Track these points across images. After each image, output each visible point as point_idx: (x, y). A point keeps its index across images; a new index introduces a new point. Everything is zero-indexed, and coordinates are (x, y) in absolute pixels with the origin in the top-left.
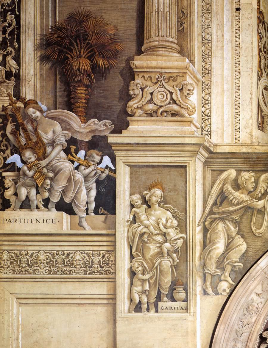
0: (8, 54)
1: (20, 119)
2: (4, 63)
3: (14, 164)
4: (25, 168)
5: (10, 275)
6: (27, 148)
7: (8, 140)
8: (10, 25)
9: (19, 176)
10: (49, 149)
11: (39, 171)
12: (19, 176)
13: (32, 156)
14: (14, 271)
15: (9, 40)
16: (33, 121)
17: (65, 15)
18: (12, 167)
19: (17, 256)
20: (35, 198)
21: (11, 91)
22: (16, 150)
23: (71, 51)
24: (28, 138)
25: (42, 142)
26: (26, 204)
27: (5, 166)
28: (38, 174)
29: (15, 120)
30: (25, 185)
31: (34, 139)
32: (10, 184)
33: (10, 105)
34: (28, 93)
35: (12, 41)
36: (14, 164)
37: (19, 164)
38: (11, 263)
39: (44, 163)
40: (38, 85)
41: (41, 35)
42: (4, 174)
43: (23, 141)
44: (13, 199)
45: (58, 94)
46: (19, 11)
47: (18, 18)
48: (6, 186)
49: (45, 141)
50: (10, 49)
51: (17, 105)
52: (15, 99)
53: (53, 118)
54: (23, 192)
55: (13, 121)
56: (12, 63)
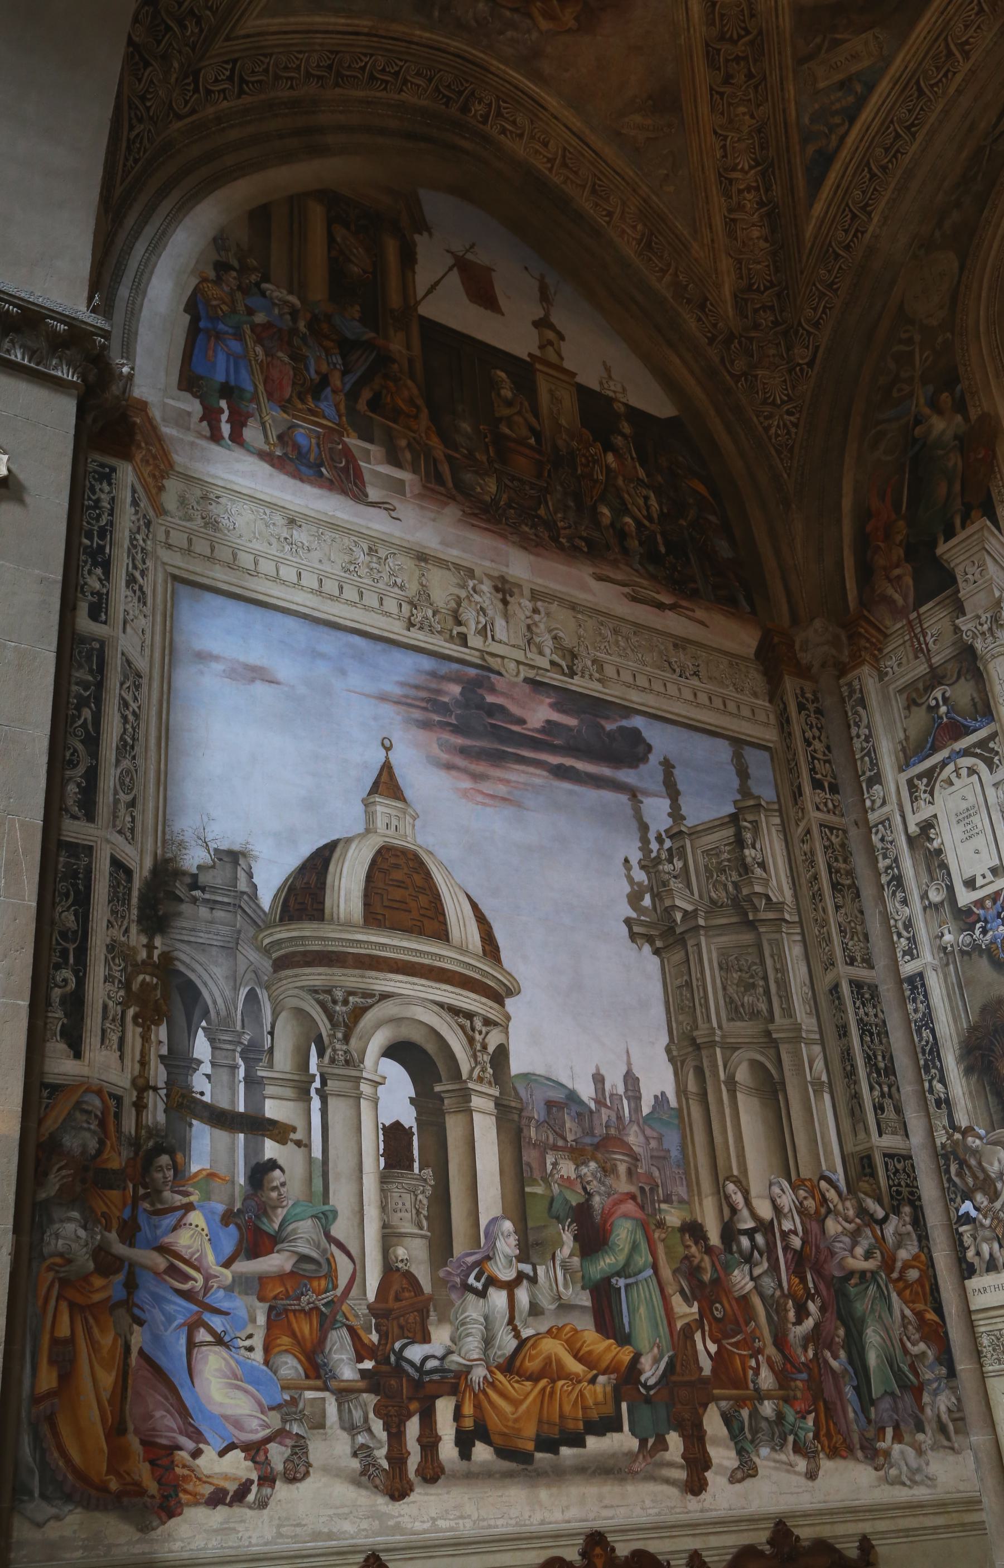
0: (933, 1078)
1: (961, 1156)
2: (931, 1090)
3: (967, 1213)
4: (981, 1217)
5: (997, 1367)
6: (976, 1190)
7: (955, 1185)
8: (927, 1042)
9: (976, 1229)
10: (999, 1185)
11: (995, 1217)
12: (976, 1229)
13: (984, 1199)
14: (999, 1360)
15: (930, 1060)
16: (975, 1152)
17: (978, 1010)
18: (967, 1219)
19: (998, 1339)
20: (998, 1254)
21: (946, 1122)
22: (967, 1196)
23: (993, 1051)
24: (975, 1177)
25: (989, 1176)
26: (992, 1266)
27: (959, 1218)
28: (996, 1222)
29: (956, 1158)
30: (986, 1240)
31: (981, 1176)
32: (969, 1242)
33: (948, 1139)
34: (963, 1120)
35: (933, 1061)
36: (967, 1213)
37: (973, 1213)
38: (994, 1350)
39: (998, 1205)
40: (970, 1106)
41: (960, 1043)
42: (961, 1229)
43: (970, 1181)
44: (976, 1261)
45: (992, 1111)
46: (932, 1023)
47: (933, 1031)
48: (966, 1245)
49: (993, 1175)
50: (933, 1071)
51: (955, 1137)
52: (951, 1131)
53: (995, 1143)
54: (985, 1248)
55: (955, 1159)
56: (939, 1087)
